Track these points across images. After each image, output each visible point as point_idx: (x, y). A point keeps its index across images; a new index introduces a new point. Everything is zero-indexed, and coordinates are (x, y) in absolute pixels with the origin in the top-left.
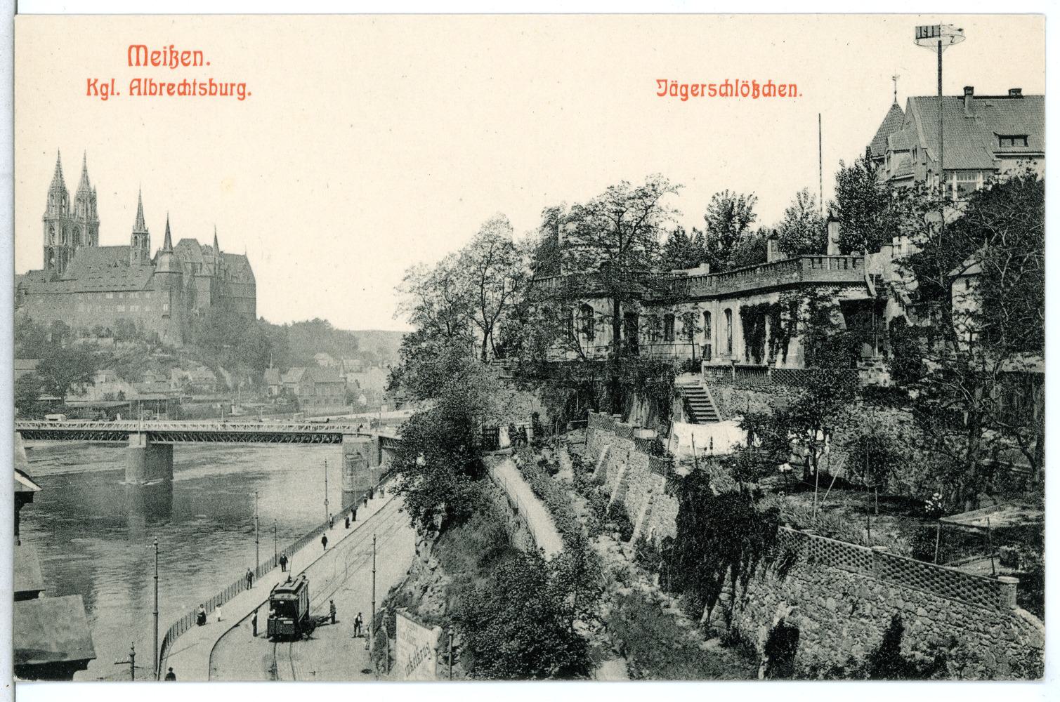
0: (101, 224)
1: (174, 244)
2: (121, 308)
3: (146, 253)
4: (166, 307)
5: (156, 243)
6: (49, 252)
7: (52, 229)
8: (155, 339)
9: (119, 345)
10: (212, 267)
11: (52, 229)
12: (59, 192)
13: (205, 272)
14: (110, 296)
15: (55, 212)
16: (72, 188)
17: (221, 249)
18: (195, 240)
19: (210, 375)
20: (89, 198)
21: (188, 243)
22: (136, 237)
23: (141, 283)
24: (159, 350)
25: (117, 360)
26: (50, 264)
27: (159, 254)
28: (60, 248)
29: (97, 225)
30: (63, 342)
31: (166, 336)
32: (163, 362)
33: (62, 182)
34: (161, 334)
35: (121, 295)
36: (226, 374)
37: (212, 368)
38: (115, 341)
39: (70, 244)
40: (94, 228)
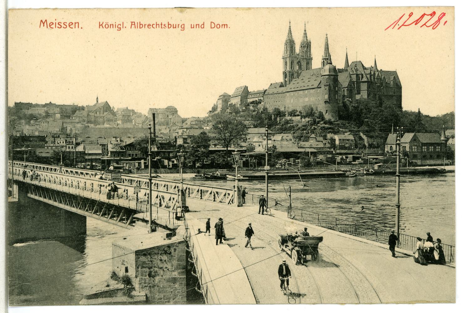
0: (313, 59)
1: (350, 63)
2: (307, 99)
4: (327, 97)
6: (285, 74)
7: (286, 63)
8: (321, 116)
9: (303, 120)
10: (368, 76)
13: (365, 79)
17: (379, 69)
19: (351, 137)
20: (307, 46)
22: (324, 61)
24: (322, 122)
25: (299, 128)
28: (290, 72)
29: (312, 59)
30: (278, 119)
31: (327, 114)
32: (323, 129)
34: (324, 113)
36: (364, 137)
37: (355, 134)
38: (301, 119)
40: (309, 60)
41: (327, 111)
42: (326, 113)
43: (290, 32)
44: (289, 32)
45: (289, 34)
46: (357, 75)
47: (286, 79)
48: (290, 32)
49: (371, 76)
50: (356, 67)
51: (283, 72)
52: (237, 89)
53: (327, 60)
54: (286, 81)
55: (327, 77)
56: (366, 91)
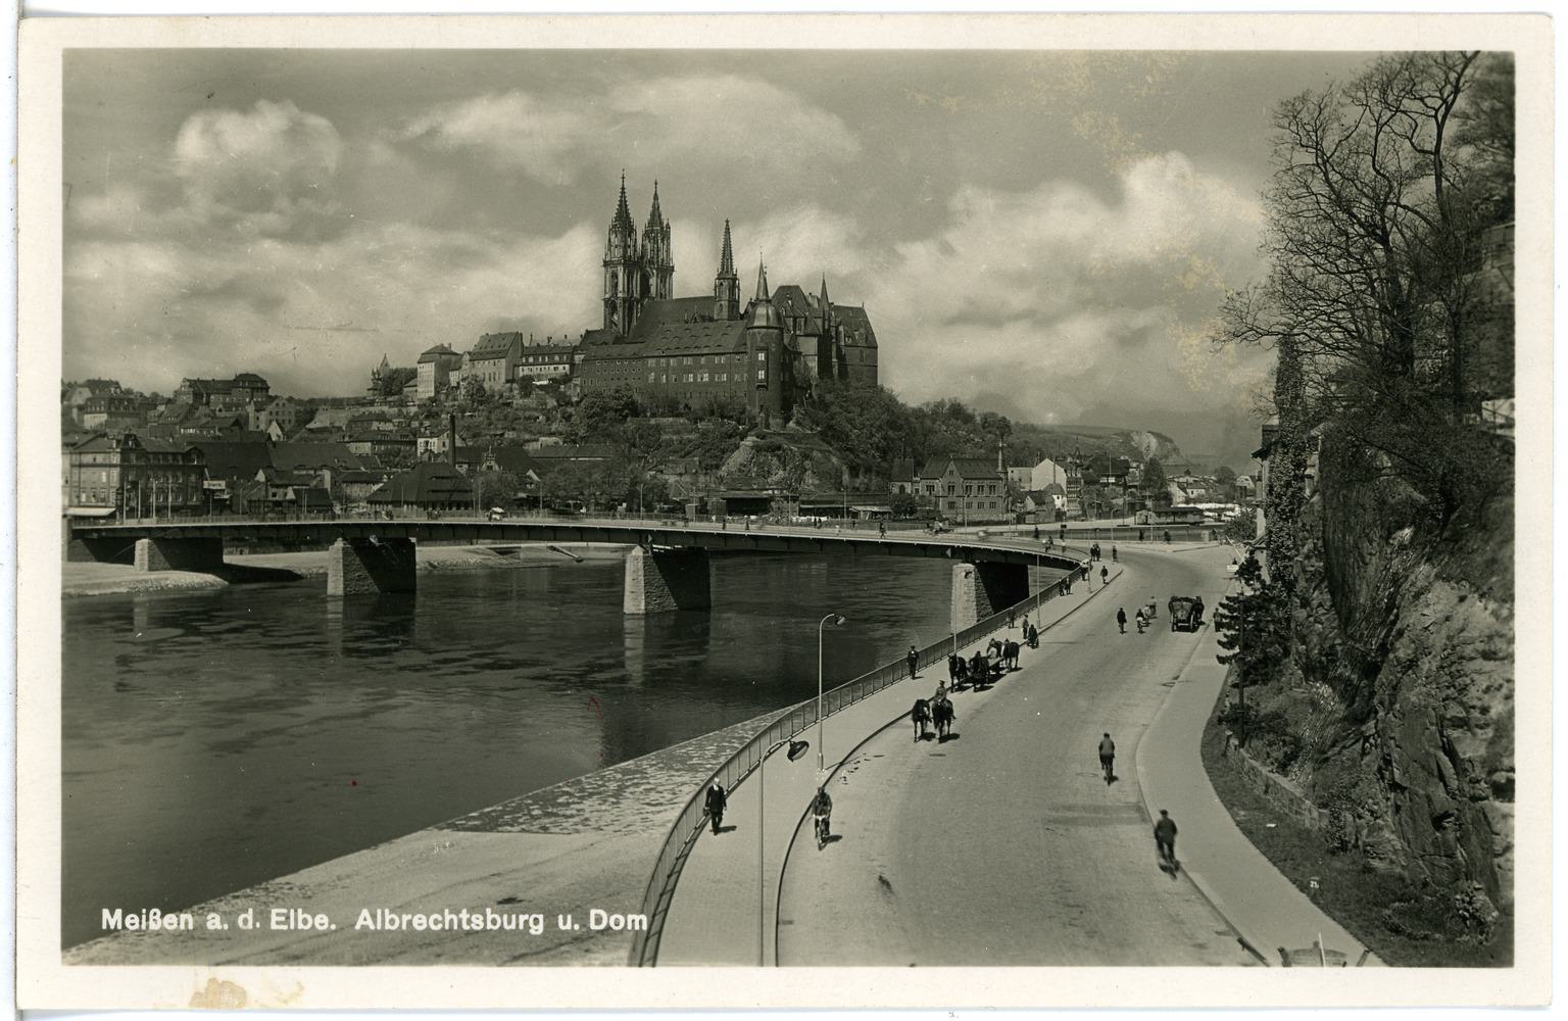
3: (734, 303)
4: (761, 374)
5: (747, 291)
6: (610, 305)
10: (819, 322)
11: (615, 276)
12: (623, 222)
14: (687, 361)
15: (618, 253)
16: (640, 219)
18: (798, 287)
21: (789, 292)
22: (721, 284)
23: (730, 343)
26: (612, 322)
27: (753, 304)
28: (624, 300)
33: (628, 214)
35: (703, 360)
39: (637, 295)
40: (666, 271)
41: (762, 406)
42: (761, 410)
43: (623, 204)
44: (621, 201)
45: (620, 206)
46: (795, 319)
47: (616, 317)
48: (623, 204)
49: (824, 323)
50: (791, 299)
51: (606, 301)
52: (487, 338)
53: (727, 278)
54: (609, 322)
55: (765, 330)
56: (816, 358)
